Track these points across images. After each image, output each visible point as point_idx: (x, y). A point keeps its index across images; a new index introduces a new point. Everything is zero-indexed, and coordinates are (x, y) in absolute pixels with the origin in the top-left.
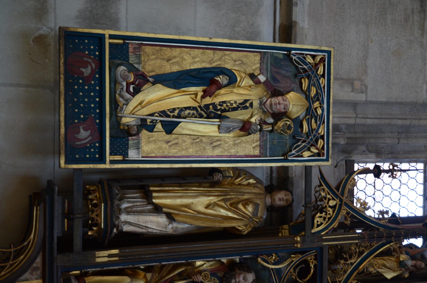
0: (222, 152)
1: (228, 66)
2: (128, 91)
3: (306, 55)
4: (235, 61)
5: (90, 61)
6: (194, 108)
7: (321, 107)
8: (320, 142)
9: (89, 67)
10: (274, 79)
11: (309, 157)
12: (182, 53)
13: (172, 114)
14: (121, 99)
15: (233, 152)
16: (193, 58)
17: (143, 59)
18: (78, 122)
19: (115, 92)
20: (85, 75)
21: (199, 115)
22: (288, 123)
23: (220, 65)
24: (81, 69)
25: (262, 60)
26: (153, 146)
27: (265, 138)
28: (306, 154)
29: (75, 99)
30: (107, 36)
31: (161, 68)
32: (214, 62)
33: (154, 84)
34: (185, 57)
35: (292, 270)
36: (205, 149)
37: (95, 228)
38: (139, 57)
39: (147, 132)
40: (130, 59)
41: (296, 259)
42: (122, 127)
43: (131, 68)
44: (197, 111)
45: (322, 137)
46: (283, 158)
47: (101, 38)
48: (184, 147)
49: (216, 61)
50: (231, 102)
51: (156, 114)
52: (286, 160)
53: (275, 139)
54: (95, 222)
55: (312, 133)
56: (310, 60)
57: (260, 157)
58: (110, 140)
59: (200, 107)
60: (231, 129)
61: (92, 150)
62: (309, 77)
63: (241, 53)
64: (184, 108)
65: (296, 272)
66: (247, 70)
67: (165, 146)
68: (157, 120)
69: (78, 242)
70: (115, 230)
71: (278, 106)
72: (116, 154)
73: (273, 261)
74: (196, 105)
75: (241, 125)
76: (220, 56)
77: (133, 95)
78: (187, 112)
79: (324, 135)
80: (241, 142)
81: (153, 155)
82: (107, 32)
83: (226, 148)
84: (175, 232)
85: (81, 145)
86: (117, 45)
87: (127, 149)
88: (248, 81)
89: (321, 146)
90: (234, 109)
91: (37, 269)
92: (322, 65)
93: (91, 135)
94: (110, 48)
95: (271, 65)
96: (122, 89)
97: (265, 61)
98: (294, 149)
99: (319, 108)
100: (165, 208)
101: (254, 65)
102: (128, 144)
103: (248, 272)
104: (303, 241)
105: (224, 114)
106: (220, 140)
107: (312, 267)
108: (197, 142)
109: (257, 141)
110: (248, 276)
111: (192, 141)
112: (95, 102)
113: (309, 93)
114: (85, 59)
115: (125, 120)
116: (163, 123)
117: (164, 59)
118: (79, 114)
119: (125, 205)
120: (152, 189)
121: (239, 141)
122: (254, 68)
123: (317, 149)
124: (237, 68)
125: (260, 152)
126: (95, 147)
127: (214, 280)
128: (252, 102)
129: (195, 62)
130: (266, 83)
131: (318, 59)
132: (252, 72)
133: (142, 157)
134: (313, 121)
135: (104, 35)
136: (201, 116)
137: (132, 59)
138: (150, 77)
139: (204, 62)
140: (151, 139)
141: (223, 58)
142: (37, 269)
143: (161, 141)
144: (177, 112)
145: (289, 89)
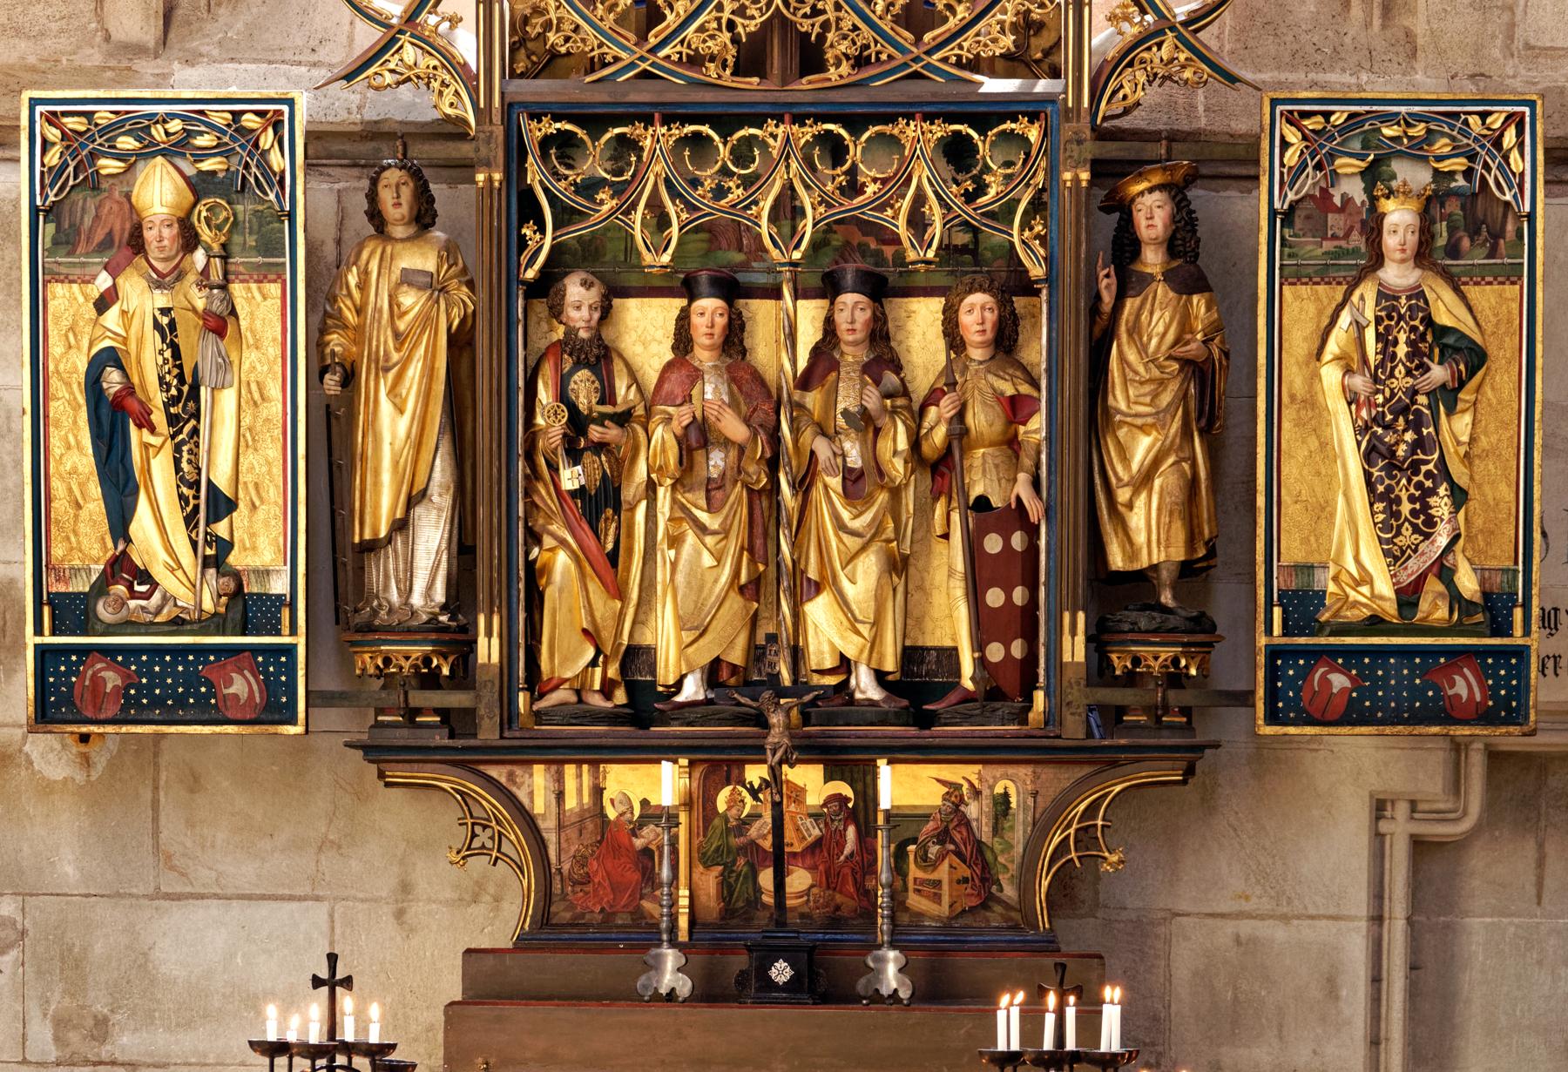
0: (274, 379)
1: (82, 366)
2: (147, 596)
3: (43, 165)
4: (70, 347)
5: (90, 672)
6: (178, 449)
7: (165, 121)
8: (250, 121)
9: (103, 674)
10: (107, 244)
11: (283, 155)
12: (60, 475)
13: (192, 502)
14: (165, 611)
15: (274, 351)
16: (69, 447)
17: (78, 562)
18: (215, 698)
19: (152, 623)
20: (119, 682)
21: (192, 438)
22: (204, 214)
23: (79, 383)
24: (108, 690)
25: (62, 277)
26: (262, 539)
27: (241, 269)
28: (277, 161)
29: (170, 702)
30: (39, 640)
31: (95, 522)
32: (75, 399)
33: (128, 540)
34: (68, 468)
35: (563, 184)
36: (267, 420)
37: (435, 662)
38: (76, 571)
39: (233, 553)
40: (81, 589)
41: (535, 174)
42: (222, 610)
43: (101, 587)
44: (183, 442)
45: (236, 115)
46: (286, 222)
47: (42, 652)
48: (264, 469)
49: (72, 393)
50: (160, 361)
51: (193, 535)
52: (291, 216)
53: (245, 243)
54: (419, 662)
55: (227, 144)
56: (53, 158)
57: (285, 281)
58: (251, 634)
59: (173, 437)
60: (220, 360)
61: (271, 669)
62: (94, 156)
63: (50, 333)
64: (177, 473)
65: (567, 172)
66: (87, 316)
67: (261, 514)
68: (206, 533)
69: (456, 699)
70: (444, 618)
71: (166, 242)
72: (279, 621)
73: (538, 236)
74: (169, 446)
75: (211, 336)
76: (59, 384)
77: (155, 585)
78: (184, 465)
79: (232, 113)
80: (252, 331)
81: (281, 540)
82: (31, 640)
83: (265, 368)
84: (448, 490)
85: (261, 692)
86: (53, 617)
87: (269, 596)
88: (112, 317)
89: (257, 119)
90: (177, 354)
91: (511, 776)
92: (65, 120)
93: (240, 672)
94: (62, 634)
95: (70, 254)
96: (143, 608)
97: (63, 270)
98: (266, 194)
99: (167, 126)
100: (395, 513)
101: (75, 299)
102: (259, 595)
103: (564, 296)
104: (488, 164)
105: (189, 379)
106: (249, 384)
107: (558, 125)
108: (254, 440)
109: (249, 288)
110: (572, 299)
111: (250, 450)
112: (174, 663)
113: (132, 155)
114: (87, 683)
115: (208, 605)
116: (211, 519)
117: (76, 516)
118: (197, 695)
119: (394, 596)
120: (357, 540)
121: (248, 334)
122: (81, 299)
123: (265, 130)
124: (85, 343)
125: (274, 281)
126: (266, 664)
127: (575, 383)
128: (160, 309)
129: (78, 443)
130: (114, 270)
131: (53, 134)
132: (91, 305)
133: (285, 564)
134: (201, 141)
135: (36, 646)
136: (195, 432)
137: (81, 586)
138: (116, 548)
139: (75, 422)
140: (248, 545)
141: (65, 376)
142: (511, 776)
143: (250, 521)
144: (185, 490)
145: (127, 206)
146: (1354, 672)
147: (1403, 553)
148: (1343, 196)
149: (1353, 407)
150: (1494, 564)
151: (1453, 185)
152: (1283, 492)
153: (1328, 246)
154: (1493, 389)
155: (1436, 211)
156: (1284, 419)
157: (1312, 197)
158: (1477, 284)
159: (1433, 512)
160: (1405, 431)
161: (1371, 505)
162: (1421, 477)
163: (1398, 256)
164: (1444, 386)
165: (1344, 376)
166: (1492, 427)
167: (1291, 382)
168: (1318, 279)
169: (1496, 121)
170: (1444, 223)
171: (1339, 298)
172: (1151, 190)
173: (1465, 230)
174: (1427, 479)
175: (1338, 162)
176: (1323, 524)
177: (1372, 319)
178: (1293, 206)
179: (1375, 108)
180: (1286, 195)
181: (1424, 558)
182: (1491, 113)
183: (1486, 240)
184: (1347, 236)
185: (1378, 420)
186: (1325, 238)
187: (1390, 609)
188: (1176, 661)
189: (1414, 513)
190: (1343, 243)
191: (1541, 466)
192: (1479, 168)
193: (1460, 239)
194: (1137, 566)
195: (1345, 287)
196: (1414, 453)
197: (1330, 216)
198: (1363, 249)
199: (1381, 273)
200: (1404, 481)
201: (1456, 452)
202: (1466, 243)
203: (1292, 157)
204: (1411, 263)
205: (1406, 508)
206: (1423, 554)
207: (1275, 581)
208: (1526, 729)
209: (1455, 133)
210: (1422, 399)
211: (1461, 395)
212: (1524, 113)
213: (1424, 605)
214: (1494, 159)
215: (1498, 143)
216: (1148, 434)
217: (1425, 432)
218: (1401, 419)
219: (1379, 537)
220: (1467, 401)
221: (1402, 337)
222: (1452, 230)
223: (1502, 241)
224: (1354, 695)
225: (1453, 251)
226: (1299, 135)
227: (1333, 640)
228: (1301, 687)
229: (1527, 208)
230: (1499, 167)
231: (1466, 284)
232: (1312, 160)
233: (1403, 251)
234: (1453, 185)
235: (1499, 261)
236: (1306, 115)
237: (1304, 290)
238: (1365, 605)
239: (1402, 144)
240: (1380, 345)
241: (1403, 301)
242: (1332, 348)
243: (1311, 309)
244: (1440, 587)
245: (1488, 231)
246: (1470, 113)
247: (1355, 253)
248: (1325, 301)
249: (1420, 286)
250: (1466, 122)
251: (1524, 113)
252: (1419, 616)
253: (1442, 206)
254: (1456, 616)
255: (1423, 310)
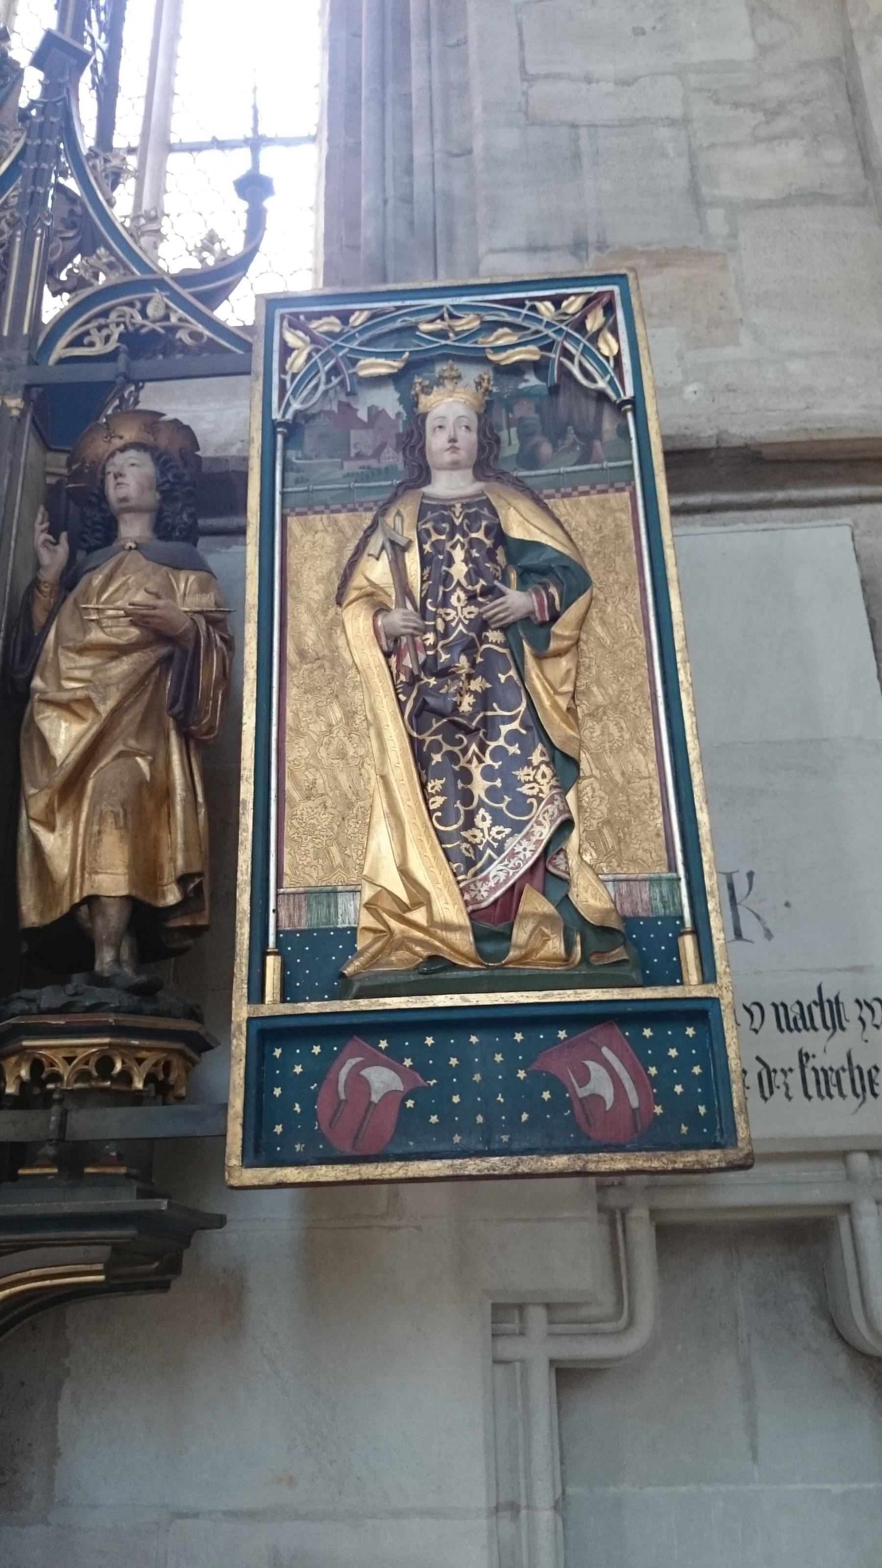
146: (408, 1062)
147: (479, 854)
148: (370, 409)
149: (393, 660)
150: (633, 872)
151: (522, 385)
152: (288, 785)
153: (350, 467)
154: (604, 623)
155: (500, 417)
156: (289, 684)
157: (330, 413)
158: (564, 496)
159: (525, 790)
160: (470, 677)
161: (423, 786)
162: (501, 742)
163: (448, 457)
164: (527, 620)
165: (376, 615)
166: (607, 673)
167: (301, 634)
168: (339, 507)
169: (573, 306)
170: (513, 430)
171: (368, 522)
172: (123, 449)
173: (544, 433)
174: (511, 744)
175: (361, 363)
176: (352, 827)
177: (413, 536)
178: (303, 418)
179: (408, 303)
180: (288, 404)
181: (515, 861)
182: (567, 296)
183: (574, 444)
184: (378, 453)
185: (430, 667)
186: (347, 458)
187: (464, 941)
188: (105, 1064)
189: (491, 792)
190: (373, 463)
191: (694, 713)
192: (555, 355)
193: (537, 446)
194: (56, 915)
195: (375, 513)
196: (486, 707)
197: (353, 433)
198: (401, 466)
199: (427, 490)
200: (474, 747)
201: (555, 706)
202: (546, 449)
203: (297, 362)
204: (469, 472)
205: (479, 787)
206: (513, 854)
207: (272, 917)
208: (733, 1154)
209: (519, 321)
210: (494, 636)
211: (556, 629)
212: (612, 293)
213: (520, 935)
214: (578, 342)
215: (580, 327)
216: (81, 718)
217: (503, 678)
218: (463, 660)
219: (436, 829)
220: (564, 638)
221: (459, 554)
222: (525, 435)
223: (597, 443)
224: (410, 1104)
225: (530, 459)
226: (308, 339)
227: (364, 1004)
228: (315, 1094)
229: (630, 393)
230: (585, 351)
231: (550, 497)
232: (325, 366)
233: (454, 449)
234: (522, 385)
235: (596, 466)
236: (319, 316)
237: (318, 521)
238: (420, 942)
239: (447, 337)
240: (426, 572)
241: (458, 509)
242: (358, 580)
243: (329, 541)
244: (546, 907)
245: (577, 433)
246: (542, 299)
247: (388, 472)
248: (349, 532)
249: (483, 494)
250: (533, 308)
251: (612, 293)
252: (512, 954)
253: (509, 409)
254: (578, 949)
255: (487, 518)
